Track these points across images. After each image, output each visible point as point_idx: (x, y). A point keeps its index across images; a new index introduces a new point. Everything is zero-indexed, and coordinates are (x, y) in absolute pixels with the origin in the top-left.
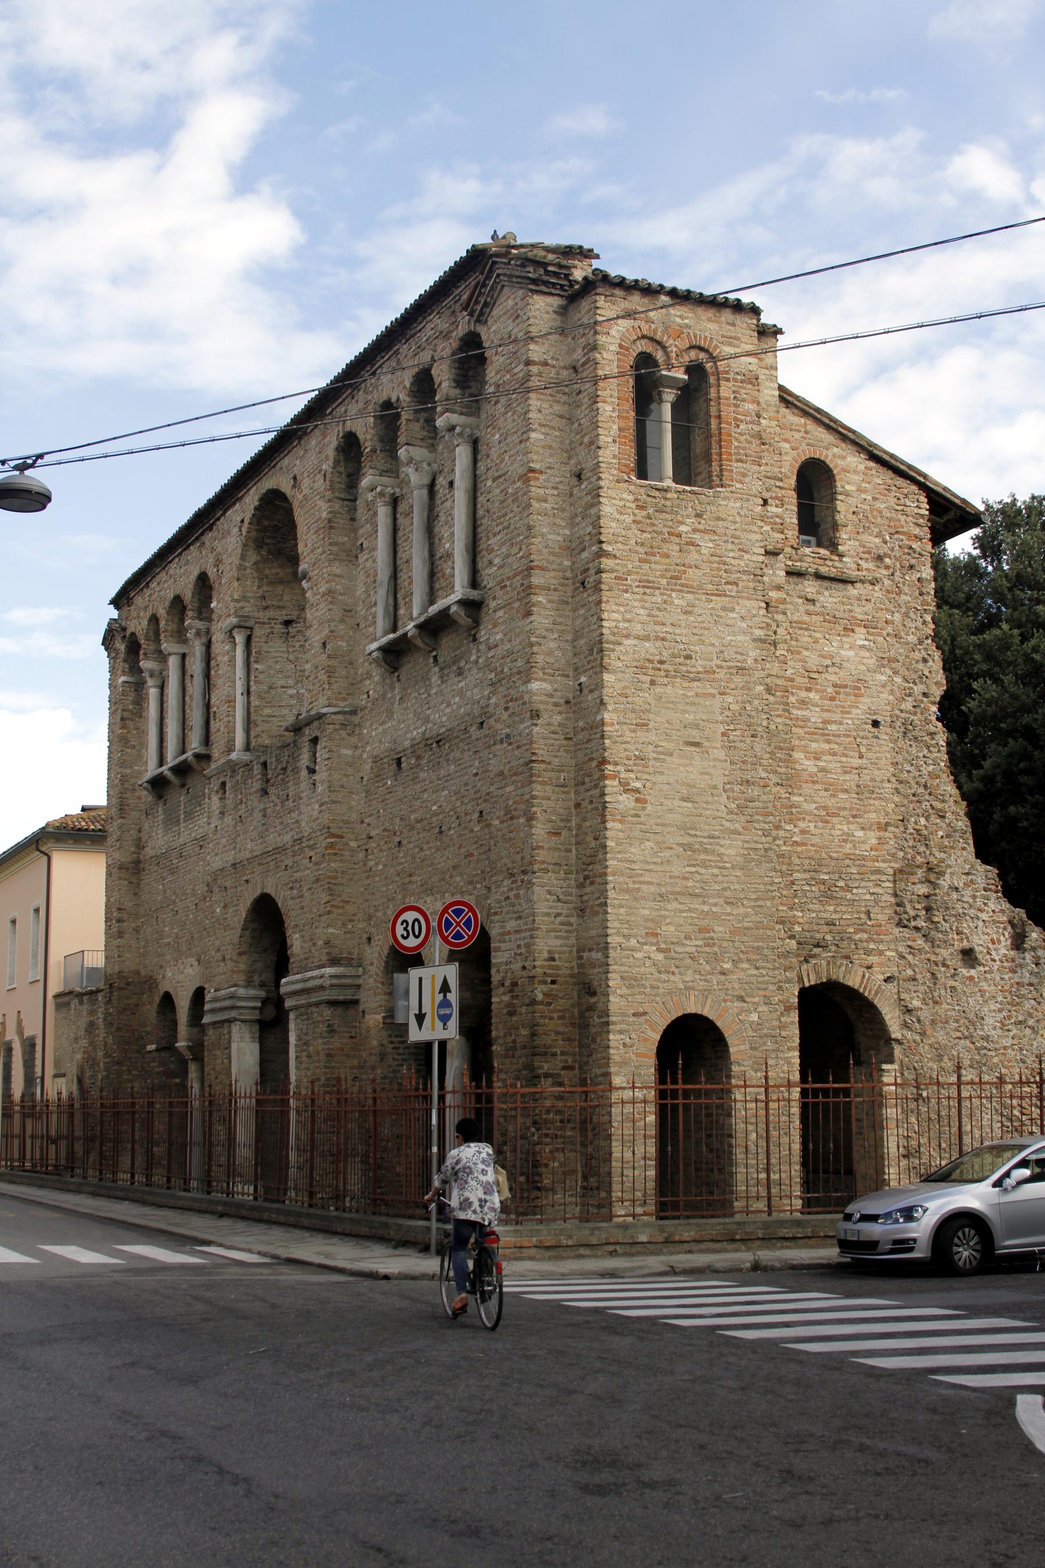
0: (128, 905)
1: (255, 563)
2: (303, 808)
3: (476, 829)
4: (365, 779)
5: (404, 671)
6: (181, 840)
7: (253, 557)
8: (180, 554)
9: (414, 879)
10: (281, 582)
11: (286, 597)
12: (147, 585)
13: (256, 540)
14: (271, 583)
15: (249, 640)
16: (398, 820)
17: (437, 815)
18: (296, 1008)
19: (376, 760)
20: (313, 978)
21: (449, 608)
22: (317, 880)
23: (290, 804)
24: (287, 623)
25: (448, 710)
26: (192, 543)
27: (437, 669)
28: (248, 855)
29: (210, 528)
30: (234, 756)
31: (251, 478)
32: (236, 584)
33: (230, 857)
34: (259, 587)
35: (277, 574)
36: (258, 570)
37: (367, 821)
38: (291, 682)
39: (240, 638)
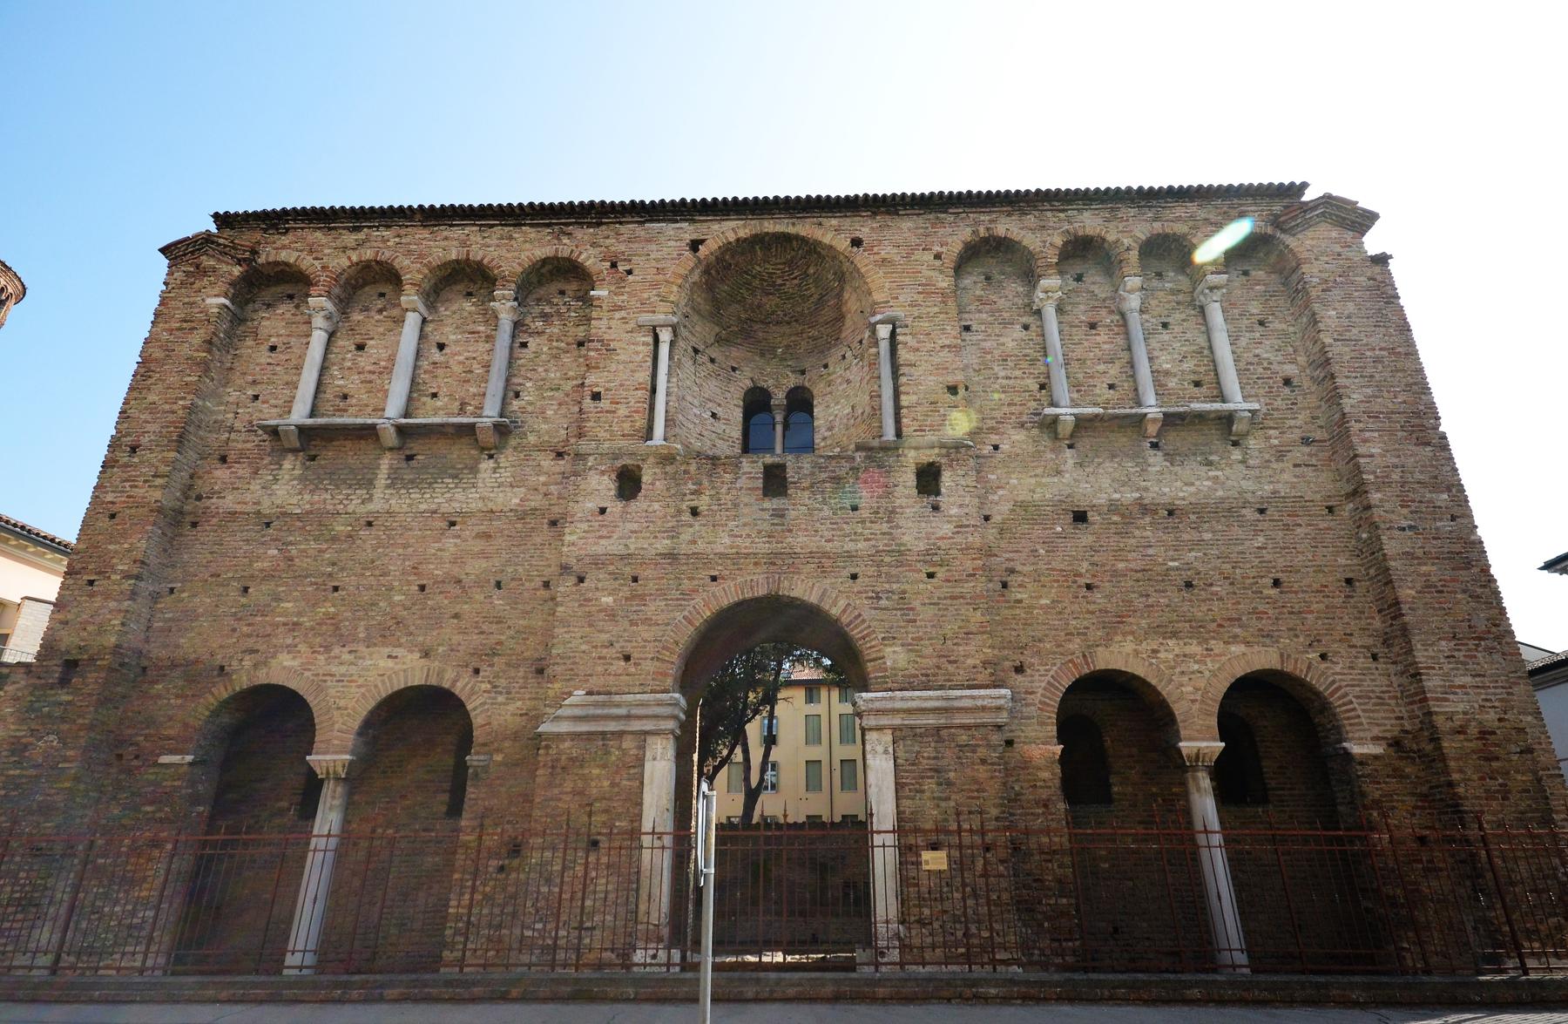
0: (153, 561)
3: (1266, 592)
4: (997, 518)
5: (1085, 443)
6: (371, 507)
7: (696, 277)
8: (492, 226)
9: (1131, 620)
10: (698, 312)
11: (698, 328)
12: (357, 229)
13: (708, 265)
15: (672, 344)
16: (1085, 565)
17: (1177, 569)
18: (894, 729)
19: (1023, 505)
20: (973, 697)
22: (953, 598)
23: (865, 514)
24: (696, 351)
25: (1192, 489)
26: (532, 225)
27: (1160, 453)
28: (721, 549)
29: (590, 225)
31: (738, 212)
32: (675, 289)
33: (663, 544)
38: (696, 402)
39: (665, 336)
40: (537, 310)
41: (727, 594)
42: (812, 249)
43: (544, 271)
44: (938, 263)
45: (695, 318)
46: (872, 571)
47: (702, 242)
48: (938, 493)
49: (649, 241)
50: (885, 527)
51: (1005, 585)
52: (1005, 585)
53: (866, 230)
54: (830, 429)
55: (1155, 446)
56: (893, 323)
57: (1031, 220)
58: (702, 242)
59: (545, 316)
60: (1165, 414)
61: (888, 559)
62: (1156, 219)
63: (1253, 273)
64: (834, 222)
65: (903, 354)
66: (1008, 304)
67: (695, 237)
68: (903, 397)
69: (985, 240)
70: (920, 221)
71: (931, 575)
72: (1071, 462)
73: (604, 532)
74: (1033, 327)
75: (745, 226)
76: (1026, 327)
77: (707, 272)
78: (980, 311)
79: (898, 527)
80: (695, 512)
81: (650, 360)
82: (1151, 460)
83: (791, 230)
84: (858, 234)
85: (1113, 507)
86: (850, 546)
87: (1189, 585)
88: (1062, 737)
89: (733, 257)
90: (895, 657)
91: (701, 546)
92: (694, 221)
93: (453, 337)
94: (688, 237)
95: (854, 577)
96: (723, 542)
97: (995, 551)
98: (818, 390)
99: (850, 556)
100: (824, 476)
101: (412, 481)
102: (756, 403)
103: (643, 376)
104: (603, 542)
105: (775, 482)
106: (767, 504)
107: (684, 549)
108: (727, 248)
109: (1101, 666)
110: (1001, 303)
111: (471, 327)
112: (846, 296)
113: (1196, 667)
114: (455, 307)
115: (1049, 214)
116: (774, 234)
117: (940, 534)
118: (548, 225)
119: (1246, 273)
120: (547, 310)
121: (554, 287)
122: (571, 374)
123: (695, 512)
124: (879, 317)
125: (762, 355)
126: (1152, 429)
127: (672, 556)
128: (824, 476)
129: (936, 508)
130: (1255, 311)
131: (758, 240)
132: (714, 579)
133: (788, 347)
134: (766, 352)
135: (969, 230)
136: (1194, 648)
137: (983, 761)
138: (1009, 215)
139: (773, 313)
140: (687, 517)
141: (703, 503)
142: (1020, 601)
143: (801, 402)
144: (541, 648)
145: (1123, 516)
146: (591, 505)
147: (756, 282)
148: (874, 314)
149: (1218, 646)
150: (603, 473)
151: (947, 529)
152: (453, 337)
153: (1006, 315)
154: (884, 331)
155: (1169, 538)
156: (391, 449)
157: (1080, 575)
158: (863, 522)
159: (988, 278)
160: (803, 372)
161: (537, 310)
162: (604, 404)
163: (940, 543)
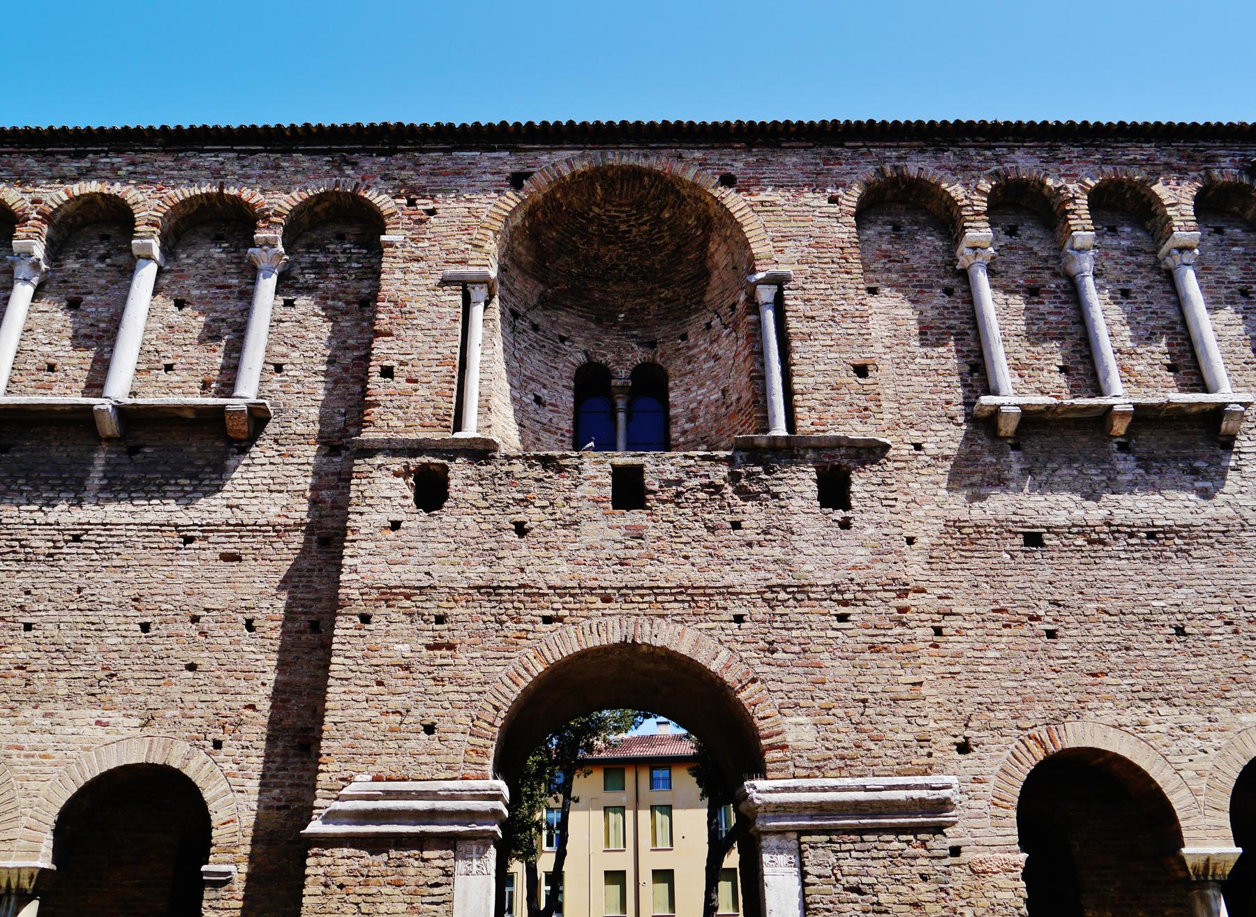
1: (515, 227)
4: (922, 541)
7: (518, 220)
11: (517, 286)
14: (512, 260)
28: (555, 580)
34: (504, 256)
35: (520, 254)
36: (511, 236)
37: (940, 592)
40: (307, 259)
41: (567, 642)
42: (668, 186)
43: (318, 209)
44: (834, 209)
45: (515, 273)
46: (761, 611)
47: (527, 175)
48: (847, 507)
49: (458, 174)
50: (778, 552)
52: (938, 631)
53: (740, 165)
54: (692, 419)
55: (1123, 447)
56: (779, 281)
57: (949, 157)
58: (527, 175)
59: (318, 267)
60: (1135, 405)
61: (782, 596)
62: (1104, 161)
63: (1228, 231)
64: (698, 154)
65: (794, 325)
66: (924, 263)
67: (517, 169)
68: (795, 380)
69: (893, 182)
70: (809, 156)
71: (842, 618)
72: (1016, 467)
73: (396, 556)
74: (958, 292)
75: (582, 157)
76: (948, 291)
77: (531, 214)
78: (889, 270)
80: (521, 529)
81: (459, 326)
82: (1120, 466)
83: (643, 163)
84: (729, 170)
86: (731, 578)
87: (1180, 631)
88: (1024, 844)
89: (565, 195)
90: (798, 731)
92: (518, 150)
93: (195, 292)
94: (508, 169)
95: (739, 619)
96: (560, 572)
97: (922, 585)
98: (675, 366)
100: (695, 482)
101: (135, 482)
102: (591, 383)
104: (396, 568)
105: (628, 491)
107: (507, 578)
108: (562, 185)
109: (1071, 744)
110: (915, 261)
111: (220, 280)
112: (712, 247)
113: (1198, 743)
114: (200, 254)
115: (972, 152)
116: (620, 168)
118: (325, 153)
119: (1219, 231)
120: (321, 258)
121: (330, 231)
122: (351, 342)
123: (521, 529)
124: (759, 276)
125: (599, 322)
126: (1120, 427)
127: (491, 591)
128: (695, 482)
129: (845, 524)
130: (1234, 278)
131: (598, 174)
132: (547, 620)
133: (632, 311)
134: (603, 317)
135: (871, 170)
136: (1191, 718)
137: (924, 878)
138: (922, 151)
139: (615, 266)
140: (512, 536)
141: (532, 516)
142: (959, 655)
143: (651, 383)
144: (306, 714)
147: (593, 228)
148: (754, 272)
149: (1223, 713)
150: (396, 475)
151: (861, 555)
152: (195, 292)
153: (923, 276)
154: (766, 294)
155: (1152, 570)
156: (109, 439)
158: (750, 544)
159: (897, 228)
160: (652, 345)
161: (307, 259)
162: (400, 383)
163: (853, 574)
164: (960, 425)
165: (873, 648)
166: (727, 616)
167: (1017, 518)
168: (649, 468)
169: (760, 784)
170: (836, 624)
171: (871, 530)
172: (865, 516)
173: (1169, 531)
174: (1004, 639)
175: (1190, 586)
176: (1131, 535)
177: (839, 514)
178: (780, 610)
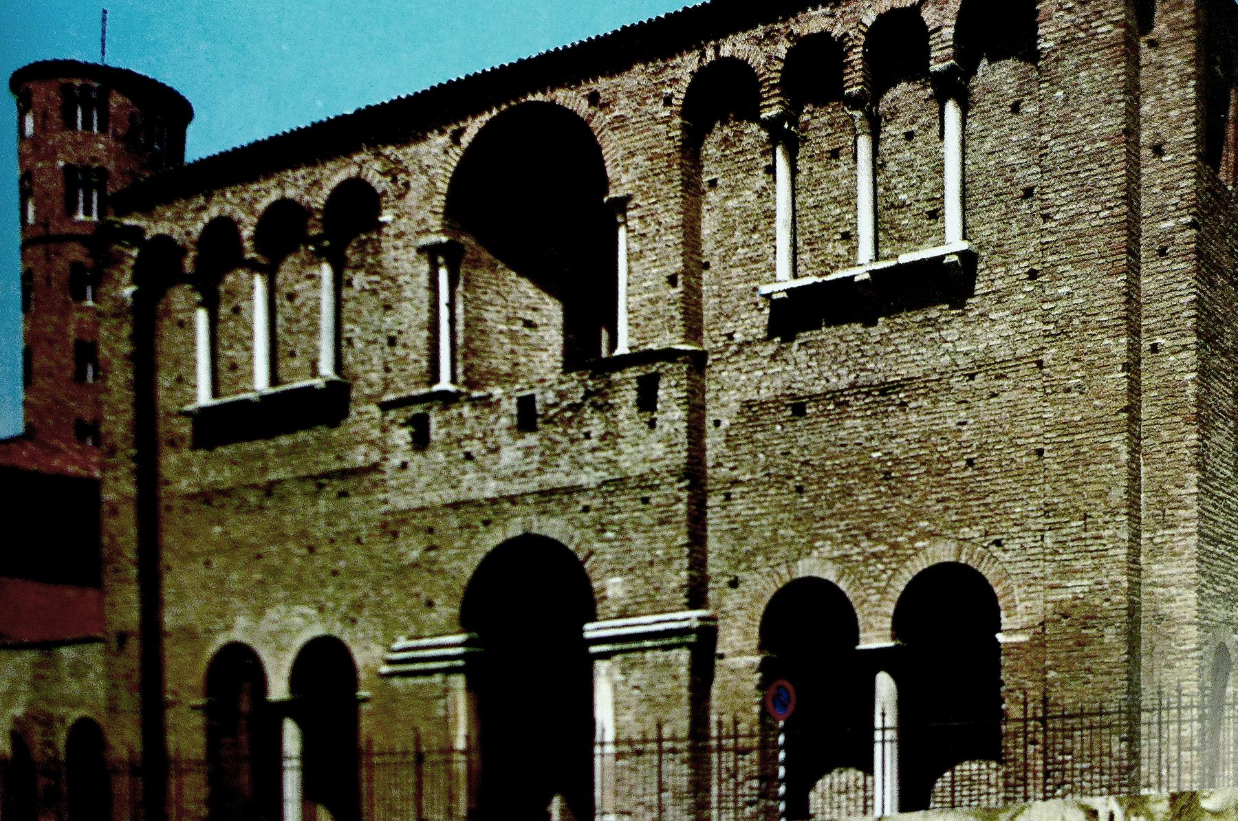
2: (622, 445)
4: (726, 423)
19: (748, 404)
21: (943, 257)
30: (436, 388)
41: (493, 539)
48: (654, 409)
50: (610, 454)
51: (728, 497)
60: (870, 272)
79: (620, 453)
85: (833, 395)
90: (614, 587)
91: (473, 495)
96: (491, 489)
99: (580, 489)
103: (425, 316)
106: (520, 443)
117: (655, 455)
129: (652, 424)
145: (838, 405)
146: (396, 461)
150: (403, 425)
157: (791, 477)
162: (400, 351)
164: (761, 310)
165: (662, 522)
166: (580, 508)
167: (788, 392)
168: (538, 398)
169: (588, 626)
170: (641, 506)
171: (667, 427)
172: (664, 416)
173: (899, 386)
174: (769, 499)
175: (902, 436)
176: (868, 394)
177: (647, 416)
178: (609, 499)
